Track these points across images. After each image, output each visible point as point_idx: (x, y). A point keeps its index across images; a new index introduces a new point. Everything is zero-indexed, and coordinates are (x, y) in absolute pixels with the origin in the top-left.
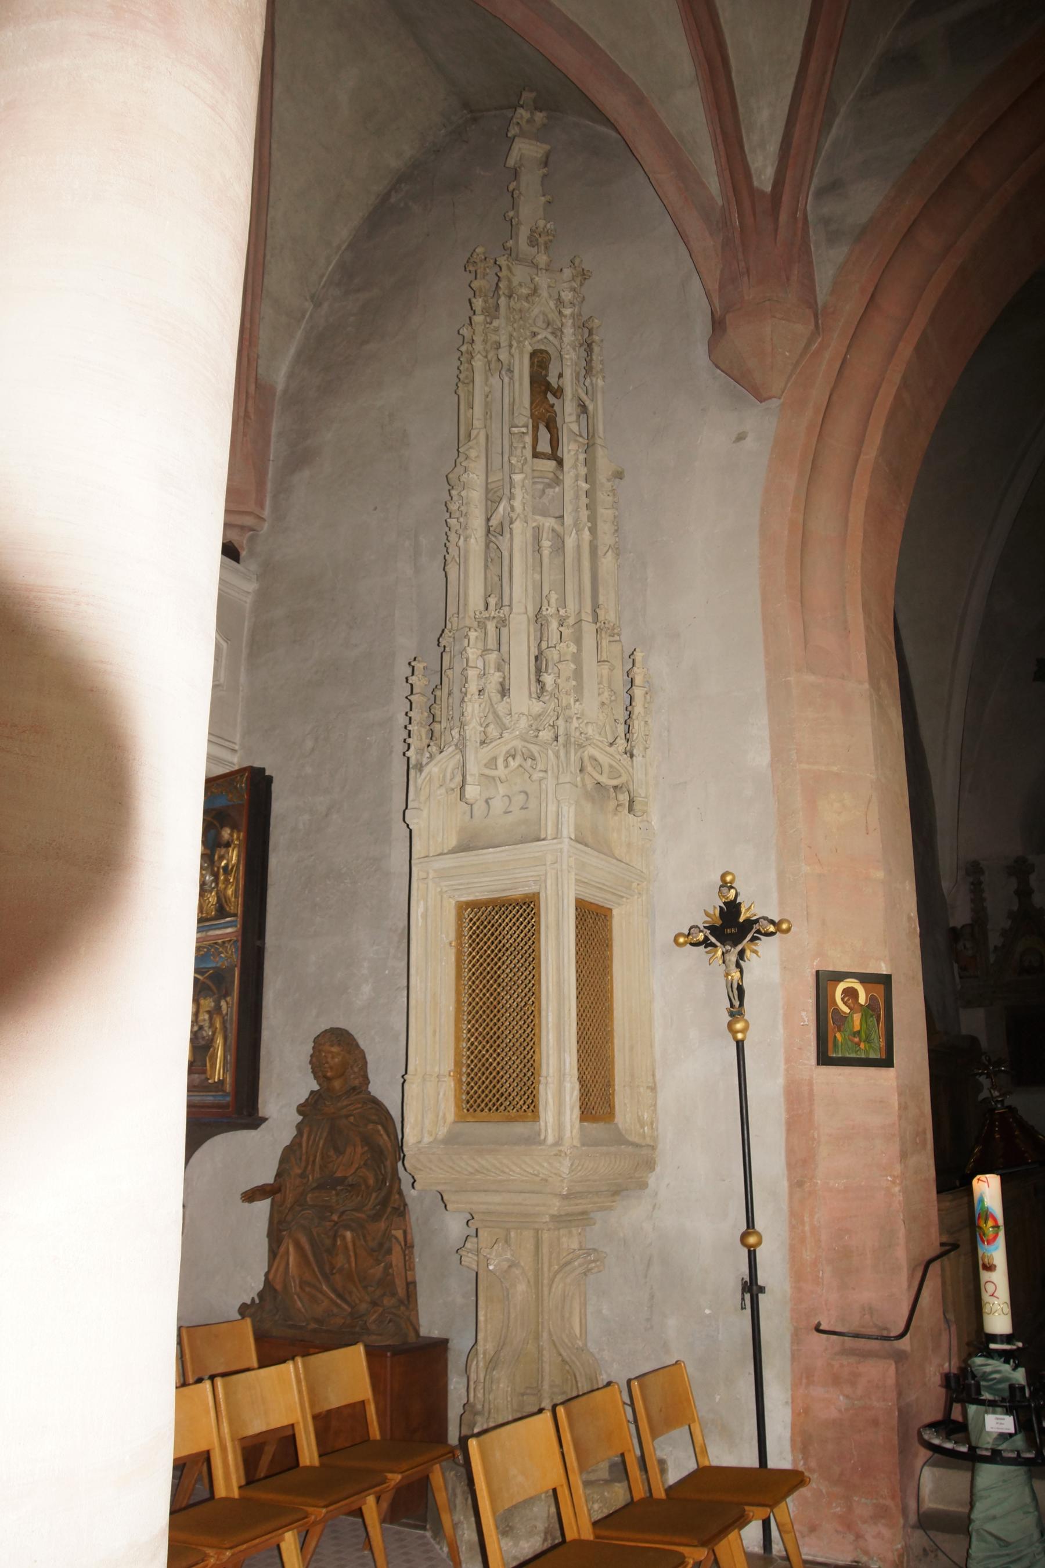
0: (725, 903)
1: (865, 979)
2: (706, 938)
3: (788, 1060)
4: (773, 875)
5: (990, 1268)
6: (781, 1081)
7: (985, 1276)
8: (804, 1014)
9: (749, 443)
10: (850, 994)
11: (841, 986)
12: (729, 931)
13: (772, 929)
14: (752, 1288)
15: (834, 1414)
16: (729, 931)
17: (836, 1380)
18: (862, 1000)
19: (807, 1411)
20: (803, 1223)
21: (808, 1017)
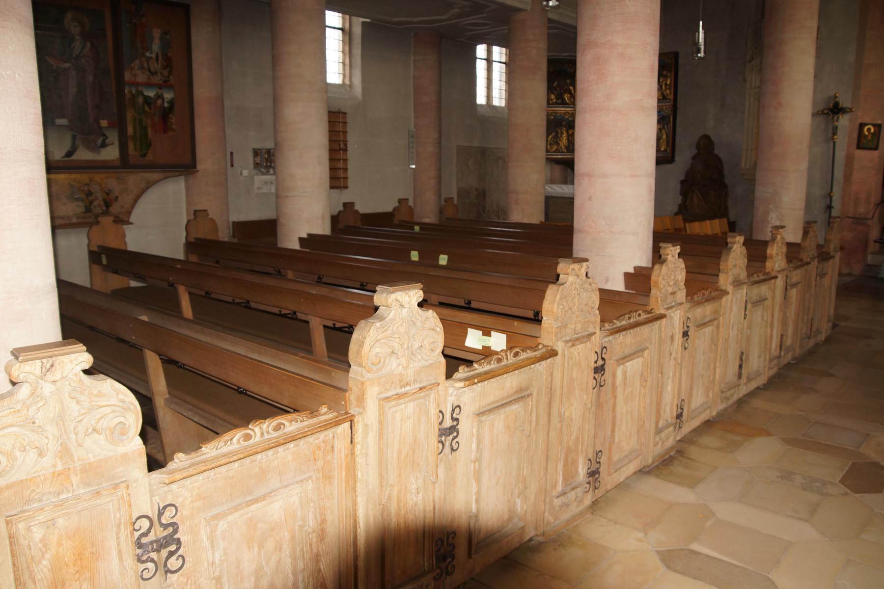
2: (828, 113)
10: (869, 130)
11: (866, 128)
13: (849, 110)
18: (872, 130)
21: (855, 135)
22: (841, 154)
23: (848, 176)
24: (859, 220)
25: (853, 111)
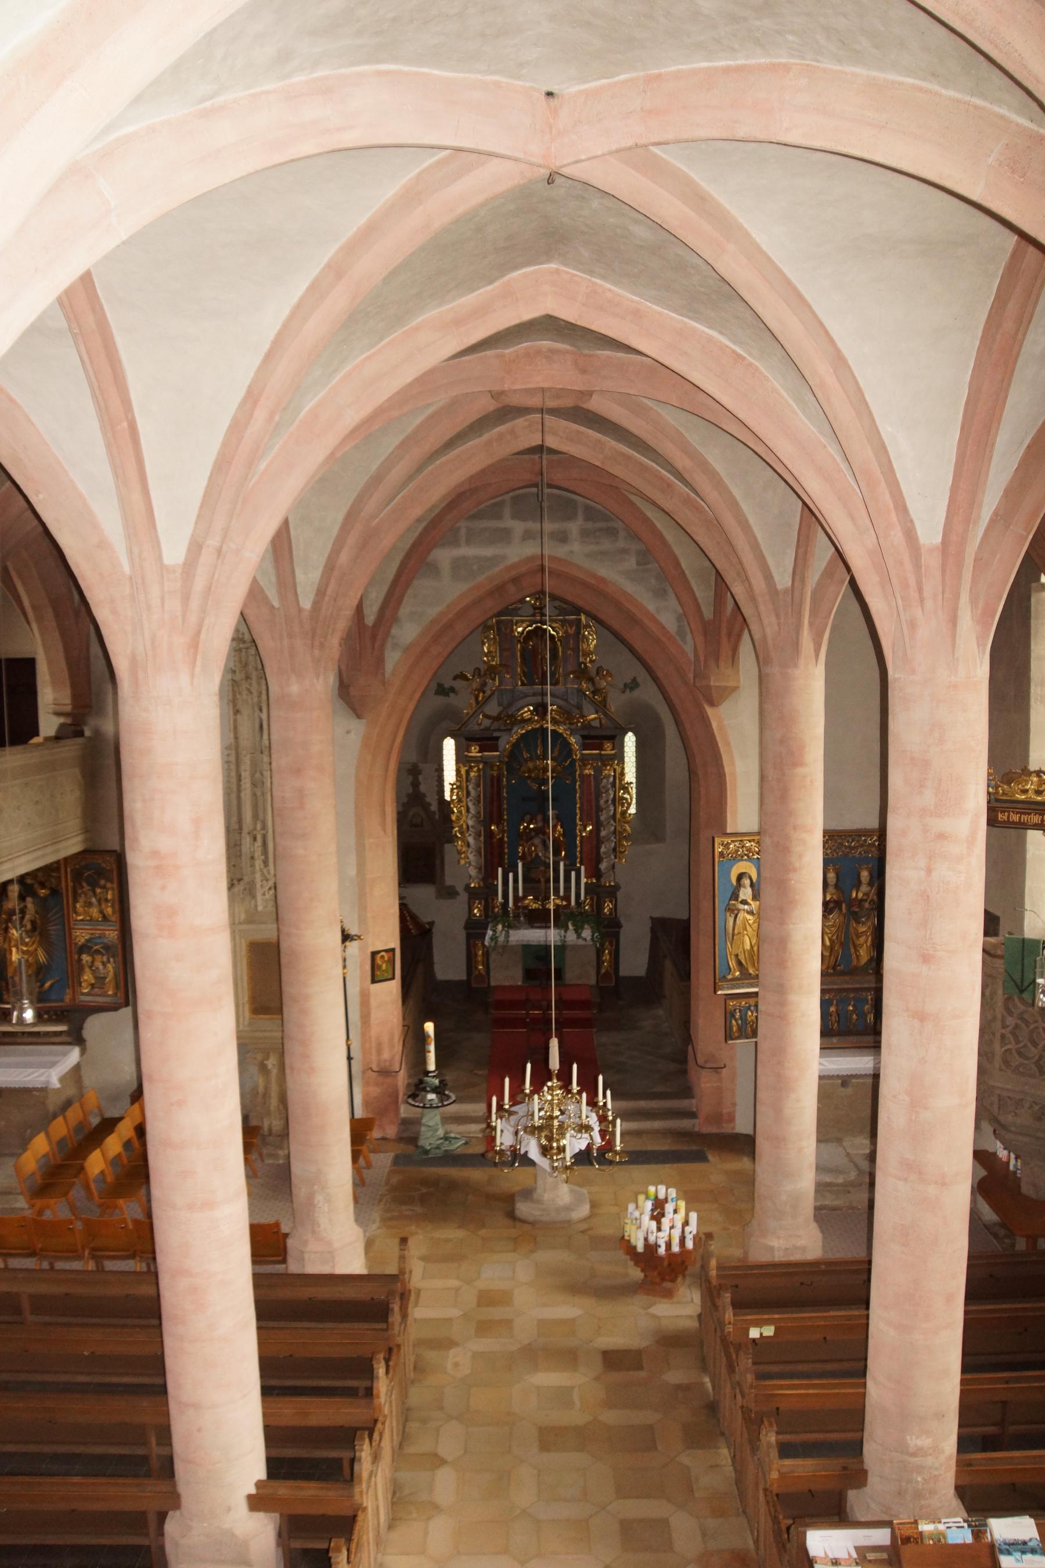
1: (386, 951)
4: (356, 916)
5: (429, 1052)
6: (358, 989)
7: (428, 1054)
9: (352, 735)
11: (380, 955)
14: (349, 1058)
15: (376, 1095)
17: (377, 1085)
21: (368, 967)
22: (354, 991)
23: (365, 1017)
24: (385, 1072)
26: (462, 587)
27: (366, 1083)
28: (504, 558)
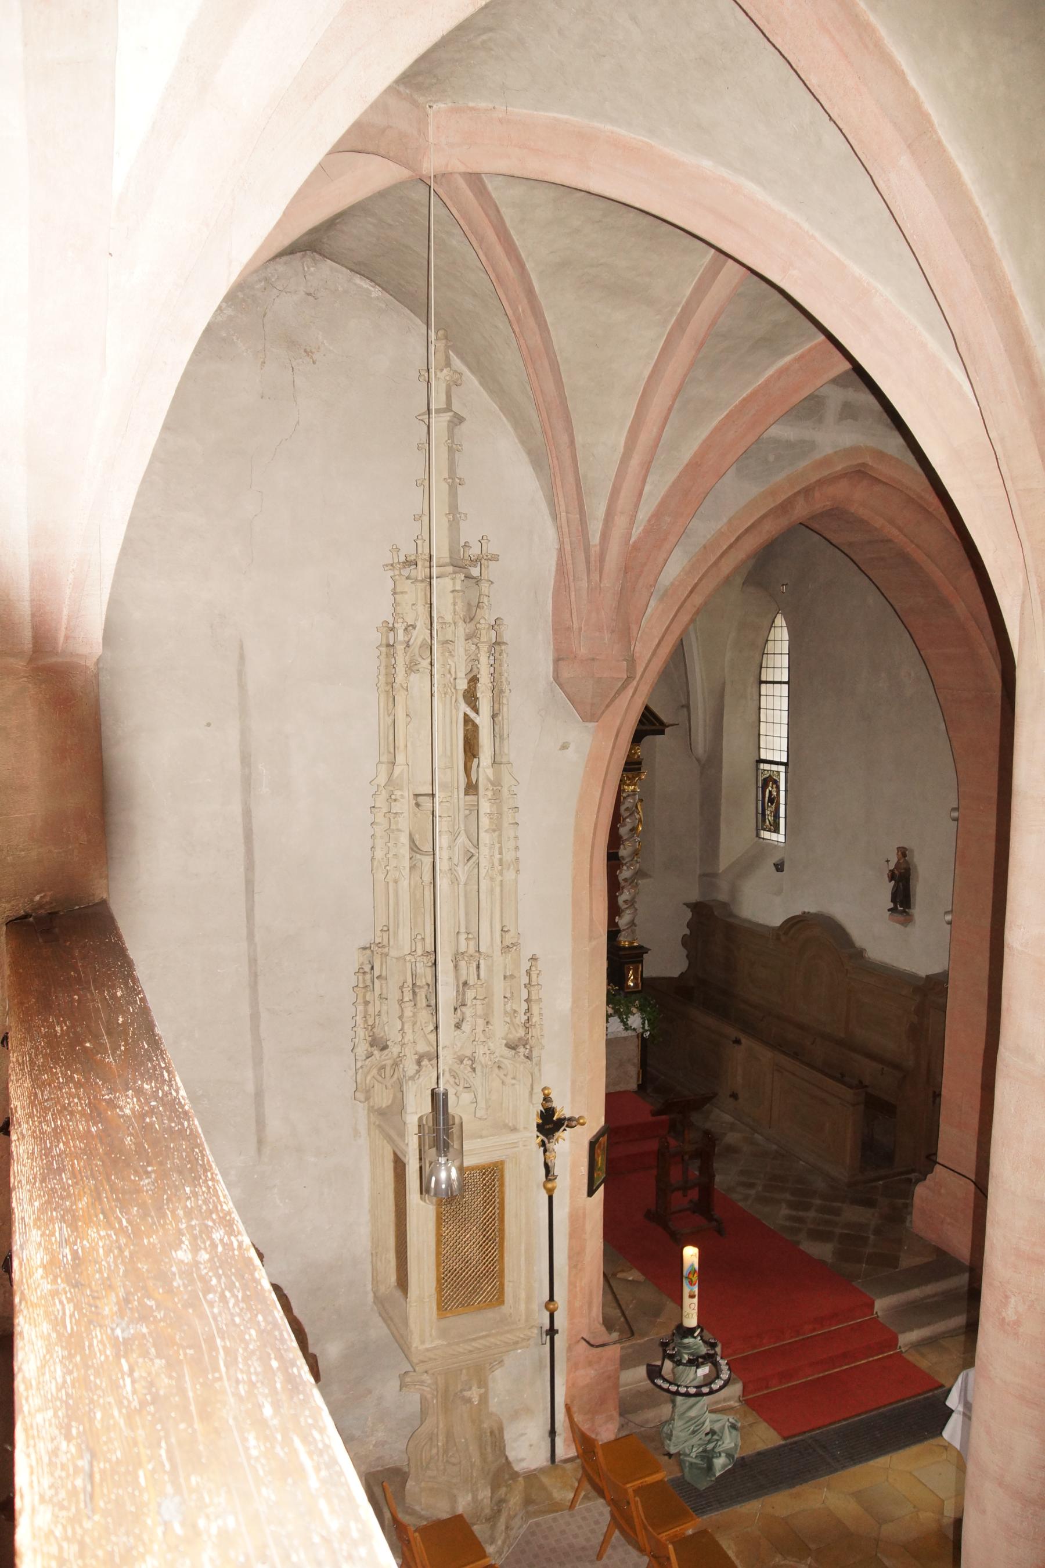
0: (545, 1110)
3: (571, 1197)
4: (569, 1083)
6: (567, 1210)
8: (582, 1168)
9: (570, 752)
12: (548, 1127)
16: (548, 1127)
17: (590, 1364)
19: (573, 1385)
20: (576, 1287)
25: (583, 1124)
26: (754, 490)
27: (573, 1366)
28: (812, 445)
